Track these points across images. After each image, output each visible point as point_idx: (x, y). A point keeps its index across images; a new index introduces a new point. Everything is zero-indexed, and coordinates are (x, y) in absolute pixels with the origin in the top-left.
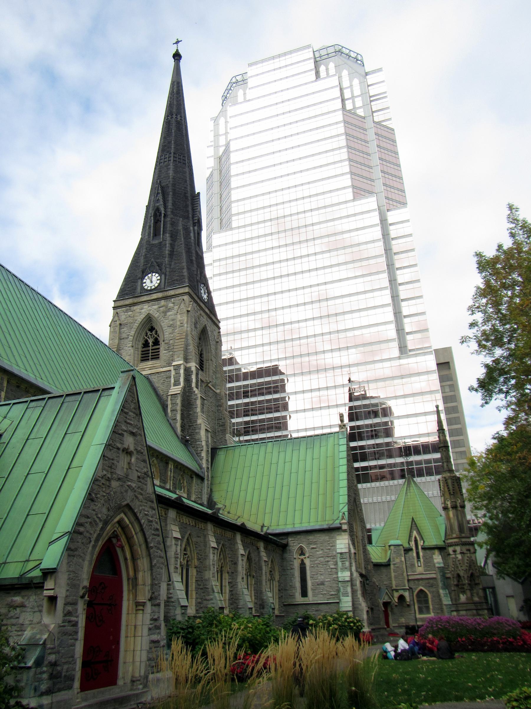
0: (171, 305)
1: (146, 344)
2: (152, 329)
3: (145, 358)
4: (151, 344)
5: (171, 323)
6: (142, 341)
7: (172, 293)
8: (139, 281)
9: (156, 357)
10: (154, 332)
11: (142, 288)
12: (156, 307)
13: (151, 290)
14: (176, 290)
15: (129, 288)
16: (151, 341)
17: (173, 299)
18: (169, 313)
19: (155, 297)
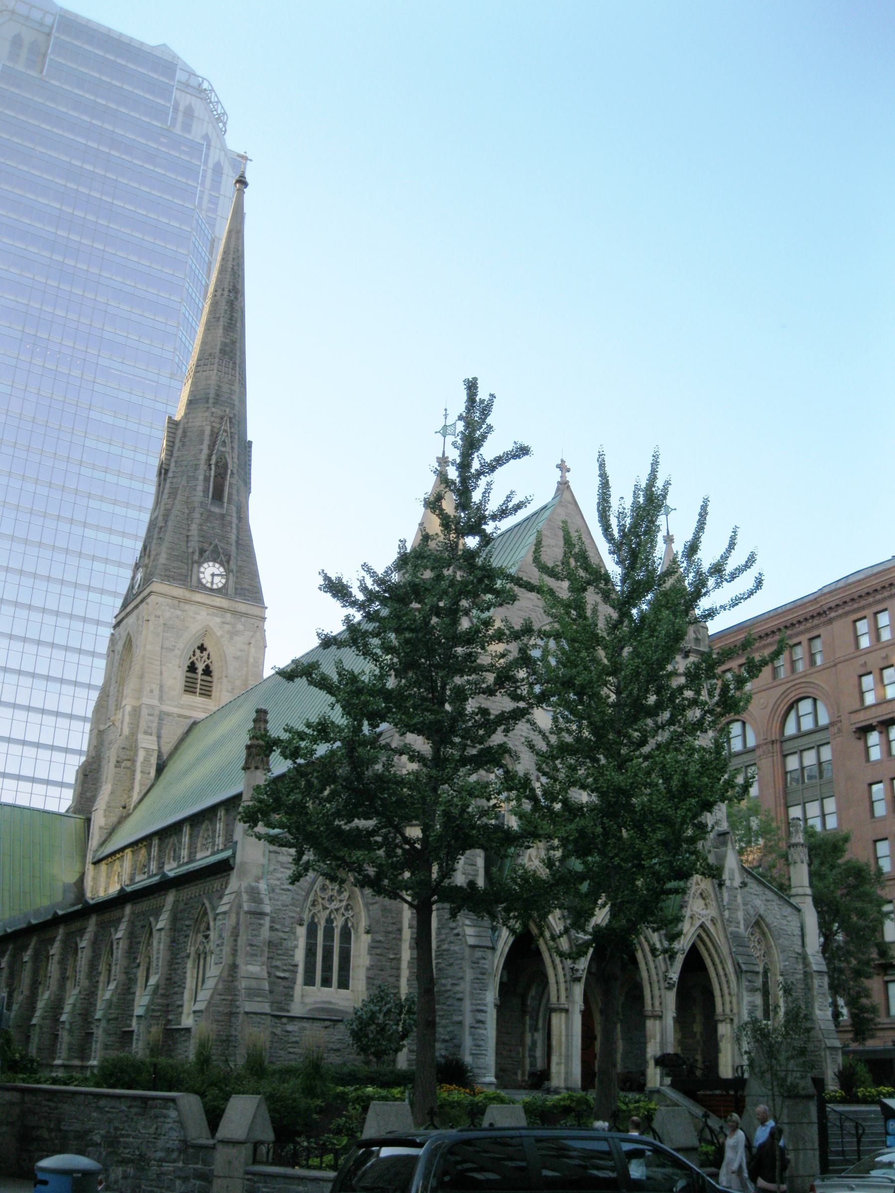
0: (240, 627)
1: (192, 668)
2: (202, 648)
3: (190, 688)
4: (200, 671)
5: (239, 653)
6: (188, 663)
7: (242, 607)
8: (195, 566)
9: (206, 693)
10: (205, 654)
11: (199, 580)
12: (218, 620)
13: (212, 590)
14: (249, 607)
15: (174, 568)
16: (201, 667)
17: (243, 619)
18: (236, 639)
19: (218, 604)
